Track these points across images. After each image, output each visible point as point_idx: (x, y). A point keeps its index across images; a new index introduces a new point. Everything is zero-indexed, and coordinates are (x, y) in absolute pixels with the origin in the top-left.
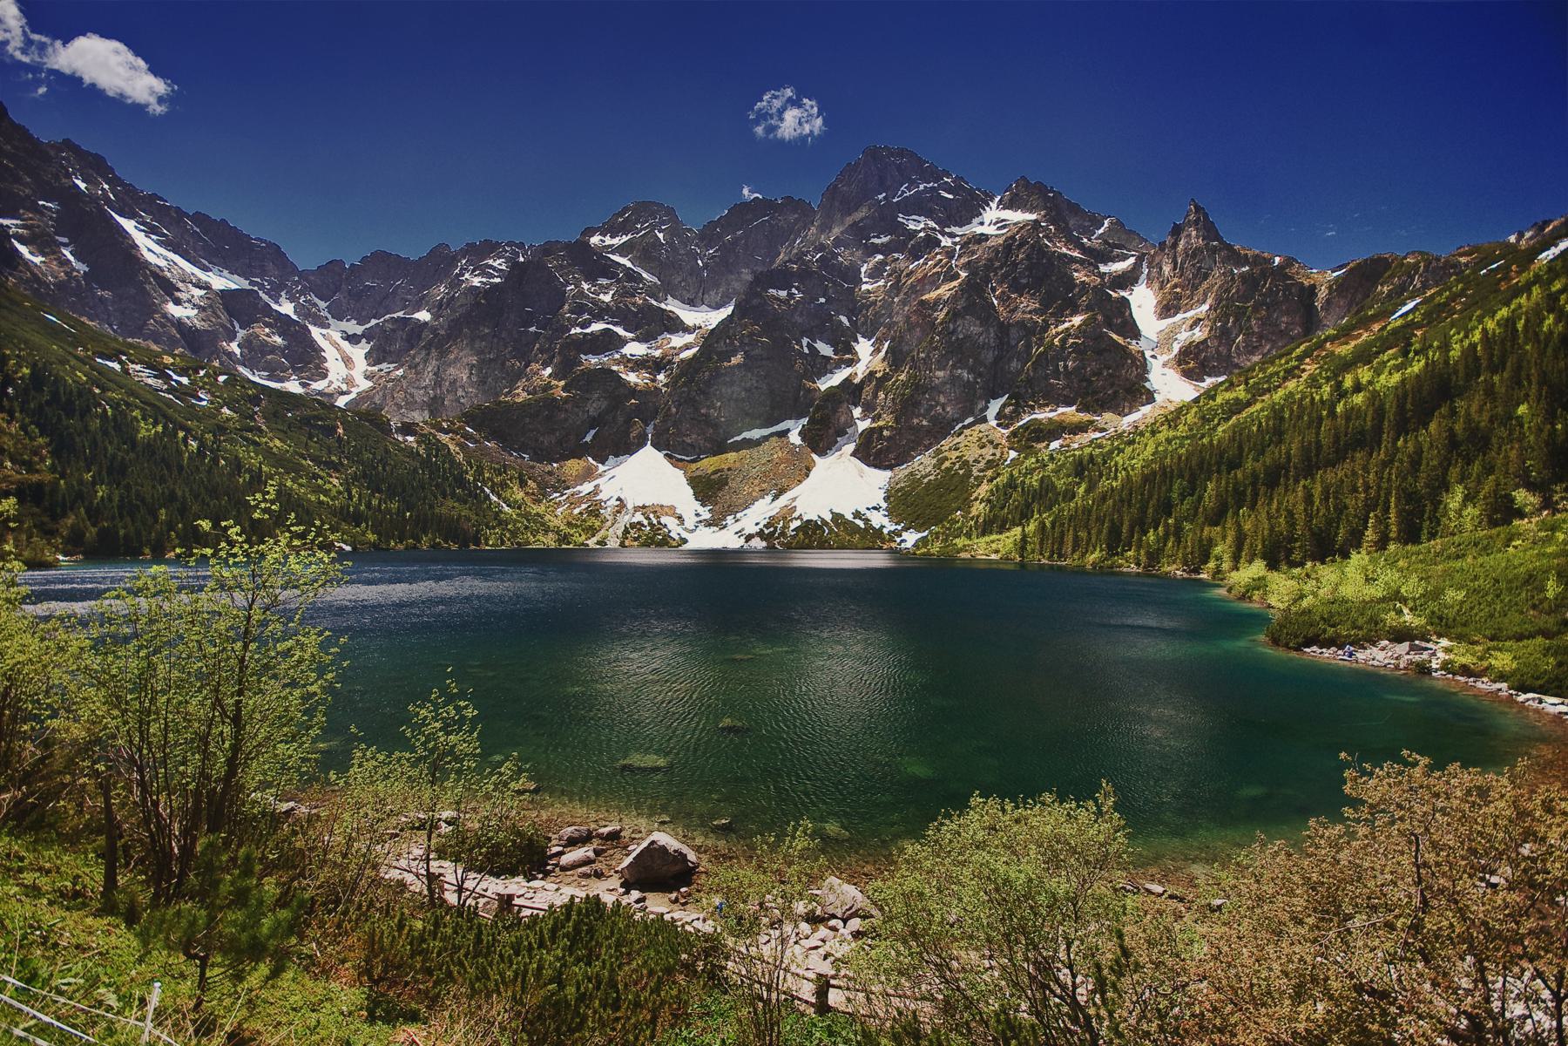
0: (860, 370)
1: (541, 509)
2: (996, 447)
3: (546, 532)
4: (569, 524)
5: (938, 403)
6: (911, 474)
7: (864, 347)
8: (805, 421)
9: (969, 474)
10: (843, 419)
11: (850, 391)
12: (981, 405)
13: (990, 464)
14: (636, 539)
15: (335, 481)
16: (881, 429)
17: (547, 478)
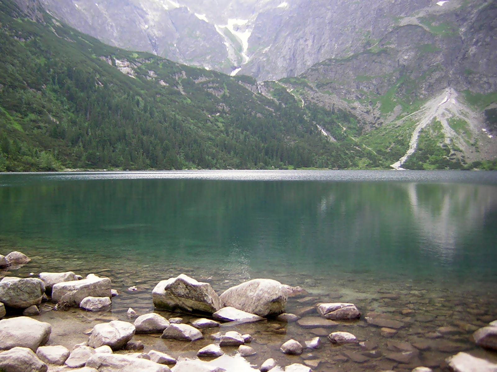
1: (356, 140)
4: (379, 152)
14: (432, 163)
15: (220, 125)
17: (365, 115)
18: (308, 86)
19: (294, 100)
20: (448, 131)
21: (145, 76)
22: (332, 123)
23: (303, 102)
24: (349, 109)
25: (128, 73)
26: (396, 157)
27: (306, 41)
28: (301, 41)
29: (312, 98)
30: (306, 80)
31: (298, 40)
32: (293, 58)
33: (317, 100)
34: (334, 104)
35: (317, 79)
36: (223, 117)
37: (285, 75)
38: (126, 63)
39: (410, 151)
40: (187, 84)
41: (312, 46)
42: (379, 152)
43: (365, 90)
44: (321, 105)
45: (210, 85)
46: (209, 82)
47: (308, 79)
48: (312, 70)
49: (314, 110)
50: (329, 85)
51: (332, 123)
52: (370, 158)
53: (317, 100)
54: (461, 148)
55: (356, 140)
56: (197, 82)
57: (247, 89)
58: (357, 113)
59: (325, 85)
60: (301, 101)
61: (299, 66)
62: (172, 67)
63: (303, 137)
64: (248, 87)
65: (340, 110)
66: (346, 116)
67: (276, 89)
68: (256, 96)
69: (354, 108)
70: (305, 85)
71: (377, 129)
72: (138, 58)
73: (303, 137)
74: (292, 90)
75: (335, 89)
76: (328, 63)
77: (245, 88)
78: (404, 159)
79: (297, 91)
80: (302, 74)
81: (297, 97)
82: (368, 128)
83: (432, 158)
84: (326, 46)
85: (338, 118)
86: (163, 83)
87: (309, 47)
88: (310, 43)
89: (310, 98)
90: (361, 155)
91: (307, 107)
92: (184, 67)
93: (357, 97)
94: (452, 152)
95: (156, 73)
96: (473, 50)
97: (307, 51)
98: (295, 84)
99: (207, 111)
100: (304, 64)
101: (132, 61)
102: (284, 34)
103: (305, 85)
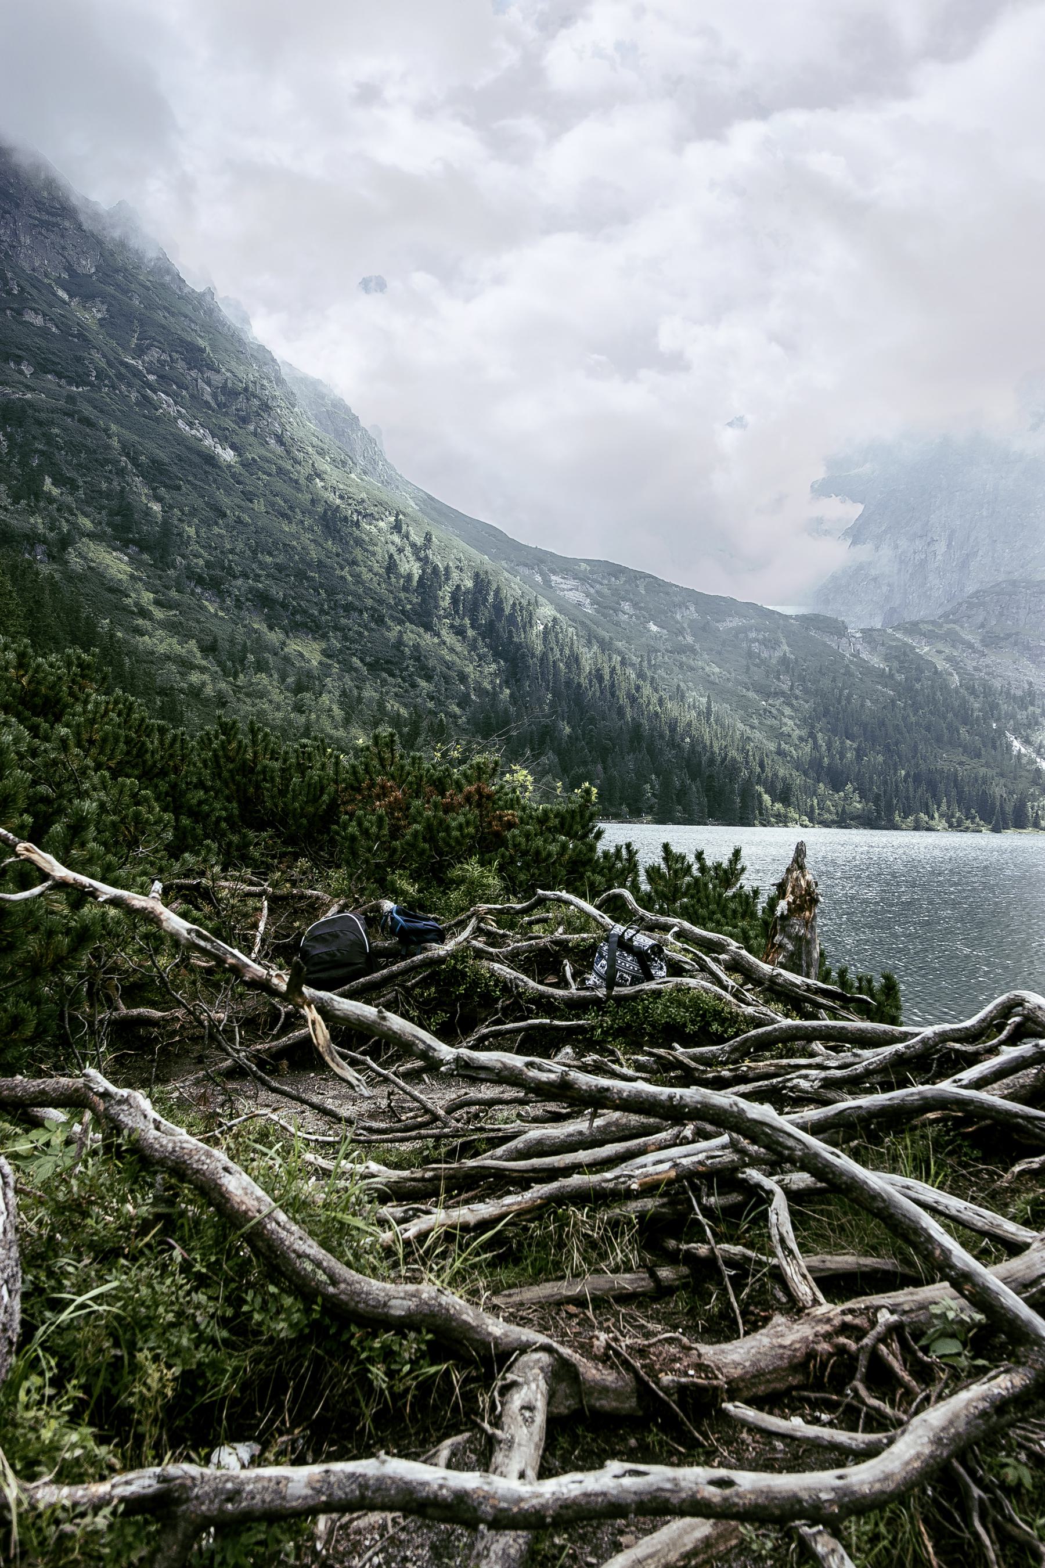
19: (936, 672)
21: (615, 611)
23: (956, 677)
25: (579, 604)
29: (976, 669)
30: (958, 628)
33: (988, 674)
34: (1030, 684)
35: (982, 626)
36: (791, 706)
38: (574, 583)
40: (702, 630)
45: (753, 635)
46: (751, 629)
47: (962, 627)
48: (971, 606)
50: (1012, 640)
53: (988, 674)
56: (721, 626)
57: (829, 646)
59: (1003, 639)
60: (951, 675)
62: (667, 594)
63: (978, 756)
64: (832, 642)
67: (890, 647)
68: (851, 661)
70: (953, 639)
72: (592, 572)
73: (978, 756)
74: (927, 649)
75: (1028, 648)
77: (825, 644)
79: (939, 652)
80: (946, 615)
81: (941, 665)
84: (980, 553)
86: (653, 628)
87: (939, 557)
88: (941, 548)
89: (970, 668)
92: (693, 596)
95: (635, 605)
98: (930, 637)
99: (757, 692)
101: (582, 579)
103: (953, 639)
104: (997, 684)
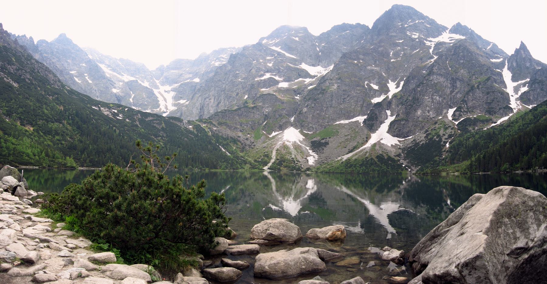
0: (390, 94)
1: (241, 154)
2: (452, 129)
3: (246, 163)
4: (255, 161)
5: (425, 110)
6: (414, 140)
7: (392, 86)
8: (365, 117)
9: (441, 140)
10: (383, 116)
11: (387, 104)
12: (445, 111)
13: (450, 136)
14: (285, 167)
16: (400, 120)
18: (213, 124)
20: (294, 152)
22: (227, 144)
24: (236, 137)
26: (266, 164)
27: (210, 99)
28: (207, 100)
31: (205, 99)
32: (202, 108)
37: (197, 118)
39: (273, 161)
41: (214, 102)
42: (255, 161)
43: (245, 127)
44: (220, 134)
49: (216, 136)
51: (227, 144)
52: (251, 164)
54: (300, 160)
55: (241, 154)
58: (241, 139)
61: (206, 113)
65: (231, 138)
66: (235, 141)
69: (239, 137)
71: (253, 148)
75: (228, 126)
76: (224, 112)
78: (270, 164)
82: (247, 147)
83: (284, 164)
85: (230, 142)
88: (212, 101)
90: (245, 162)
91: (213, 136)
93: (241, 131)
94: (296, 162)
96: (305, 110)
97: (210, 105)
100: (209, 112)
102: (197, 96)
104: (220, 134)
